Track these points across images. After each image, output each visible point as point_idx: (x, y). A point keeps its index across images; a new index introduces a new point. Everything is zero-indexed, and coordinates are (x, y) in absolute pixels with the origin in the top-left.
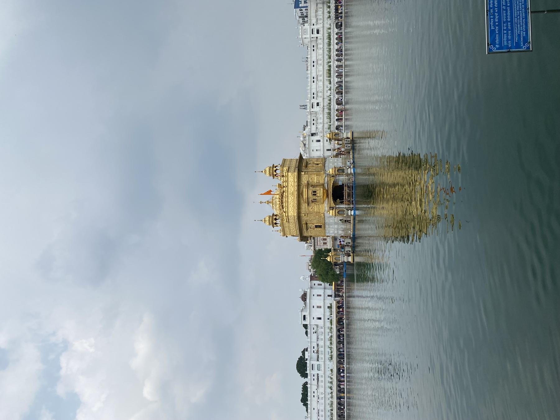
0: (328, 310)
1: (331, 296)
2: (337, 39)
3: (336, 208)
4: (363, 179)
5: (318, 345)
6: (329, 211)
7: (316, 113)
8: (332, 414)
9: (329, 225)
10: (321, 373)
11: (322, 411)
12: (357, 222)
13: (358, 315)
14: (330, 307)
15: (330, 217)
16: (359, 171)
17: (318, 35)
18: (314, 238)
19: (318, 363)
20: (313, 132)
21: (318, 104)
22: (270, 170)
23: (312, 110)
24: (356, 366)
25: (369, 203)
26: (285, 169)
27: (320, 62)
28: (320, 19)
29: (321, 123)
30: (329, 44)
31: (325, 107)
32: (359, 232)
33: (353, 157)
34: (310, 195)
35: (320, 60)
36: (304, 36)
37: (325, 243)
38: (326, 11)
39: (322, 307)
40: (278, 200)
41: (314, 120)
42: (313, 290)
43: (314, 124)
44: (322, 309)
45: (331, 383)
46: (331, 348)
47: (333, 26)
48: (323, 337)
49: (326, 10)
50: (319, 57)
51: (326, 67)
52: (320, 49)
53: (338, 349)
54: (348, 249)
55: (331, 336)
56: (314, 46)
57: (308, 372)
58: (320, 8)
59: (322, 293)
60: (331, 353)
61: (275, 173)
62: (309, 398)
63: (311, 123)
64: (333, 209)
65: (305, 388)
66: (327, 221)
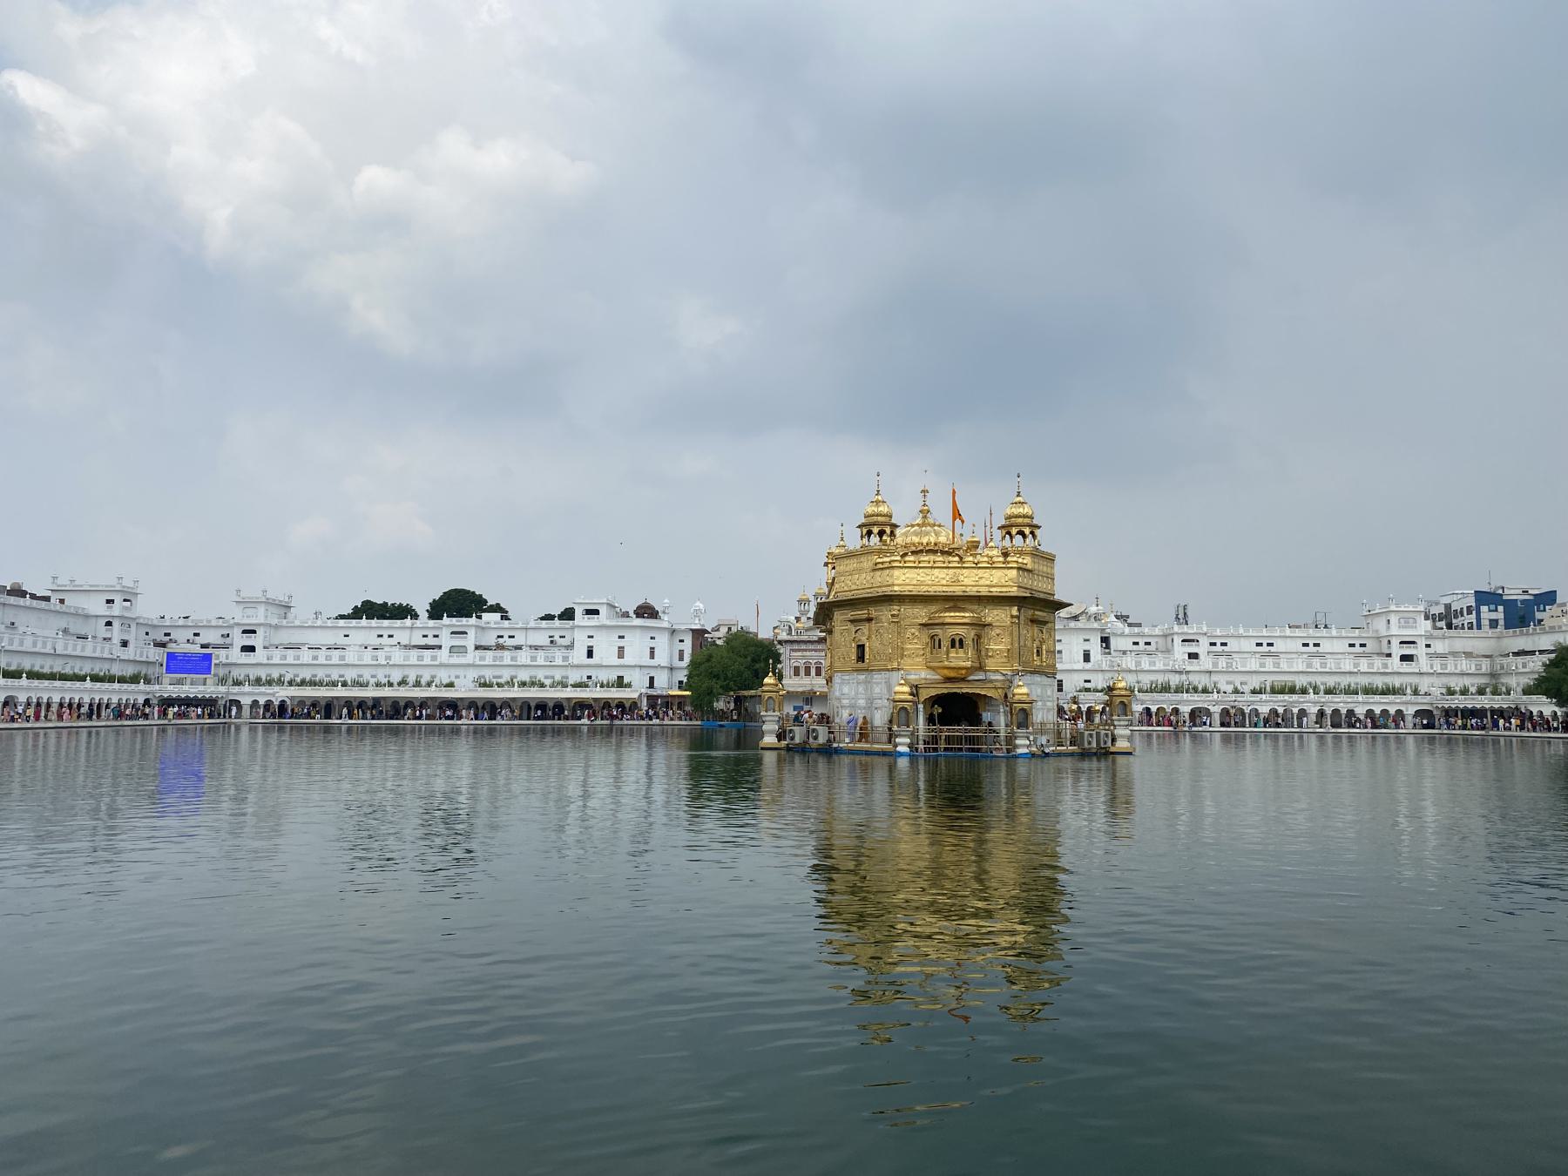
1: (651, 685)
2: (1385, 712)
3: (916, 704)
4: (997, 784)
5: (518, 648)
6: (907, 683)
7: (1168, 651)
8: (334, 684)
9: (866, 682)
10: (443, 656)
11: (342, 658)
13: (601, 757)
14: (620, 683)
15: (889, 688)
16: (1022, 768)
17: (1396, 659)
18: (822, 640)
19: (471, 648)
20: (1113, 642)
22: (1025, 516)
23: (1178, 640)
24: (463, 750)
26: (1027, 560)
27: (1317, 664)
28: (1444, 666)
29: (1138, 663)
30: (1369, 691)
31: (1184, 677)
33: (1060, 755)
35: (1323, 665)
36: (1394, 619)
37: (797, 672)
38: (1467, 681)
39: (621, 661)
40: (933, 540)
41: (1148, 644)
43: (1136, 643)
44: (616, 661)
45: (418, 684)
46: (510, 683)
47: (1423, 703)
48: (540, 661)
49: (1472, 683)
50: (1334, 661)
51: (1301, 681)
52: (1356, 665)
53: (507, 703)
55: (542, 685)
56: (1362, 645)
58: (1478, 667)
60: (499, 685)
61: (1014, 531)
62: (374, 622)
63: (1138, 635)
64: (912, 694)
65: (402, 612)
66: (877, 677)
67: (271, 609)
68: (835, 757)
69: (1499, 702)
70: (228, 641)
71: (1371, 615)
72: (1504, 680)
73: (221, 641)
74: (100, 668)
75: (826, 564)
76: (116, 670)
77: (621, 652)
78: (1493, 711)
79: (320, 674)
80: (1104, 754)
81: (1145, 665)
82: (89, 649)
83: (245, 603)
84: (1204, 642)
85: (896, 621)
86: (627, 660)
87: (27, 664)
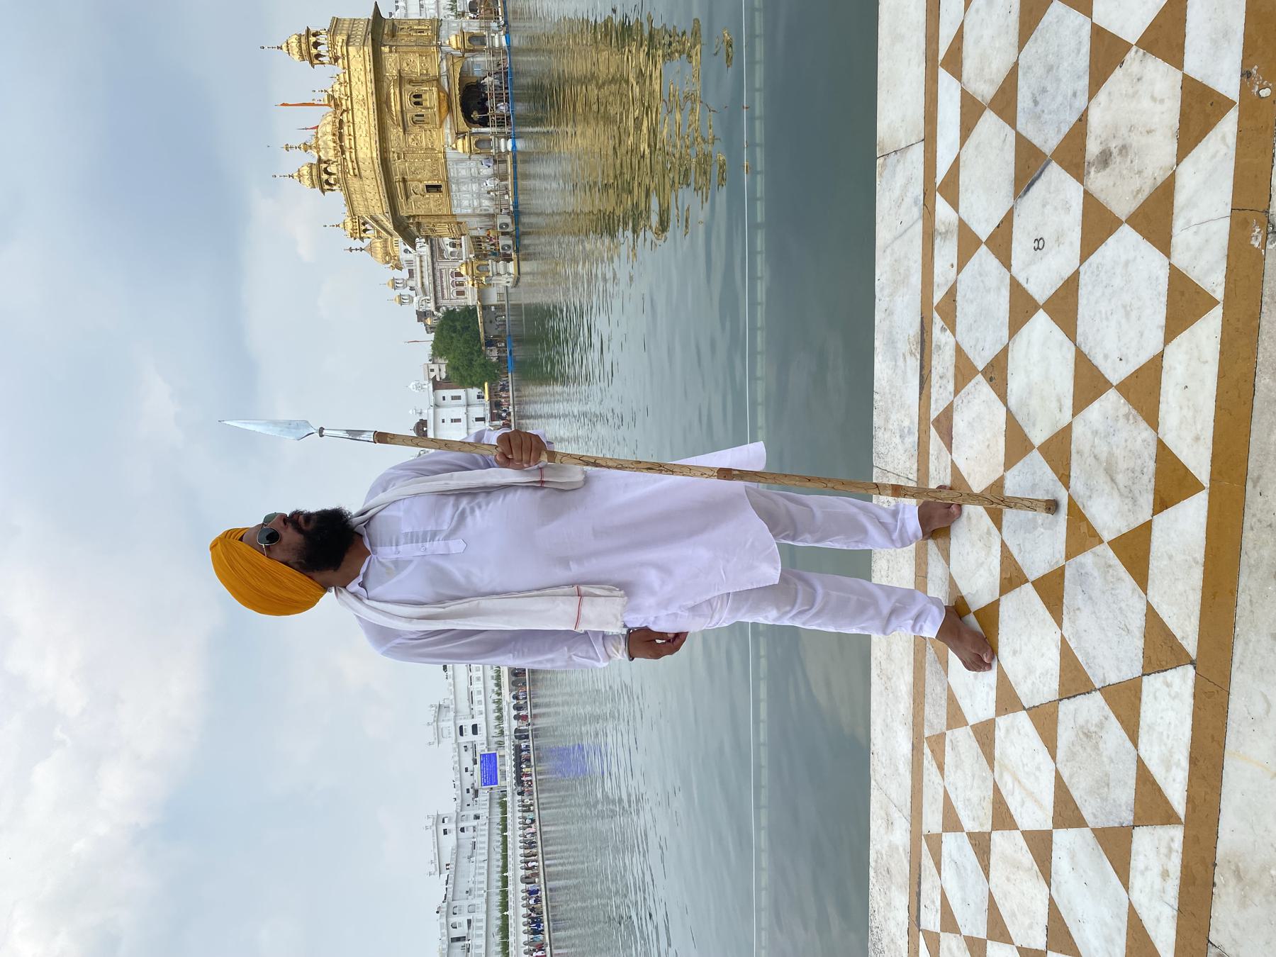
1: (483, 419)
3: (472, 134)
9: (458, 184)
18: (427, 237)
22: (300, 42)
34: (408, 104)
37: (461, 293)
40: (330, 137)
42: (439, 410)
61: (314, 51)
68: (520, 208)
70: (469, 746)
73: (470, 751)
74: (497, 829)
76: (497, 818)
82: (482, 840)
85: (402, 155)
87: (496, 876)
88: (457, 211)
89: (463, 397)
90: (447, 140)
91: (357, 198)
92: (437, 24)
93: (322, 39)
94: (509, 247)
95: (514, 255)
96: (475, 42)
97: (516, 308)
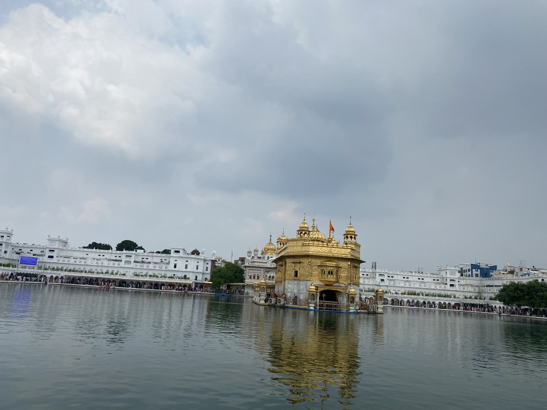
0: (182, 275)
1: (196, 279)
2: (445, 303)
3: (317, 293)
4: (342, 321)
5: (150, 263)
7: (374, 278)
8: (82, 272)
9: (298, 284)
10: (122, 264)
11: (85, 262)
12: (294, 310)
13: (176, 303)
14: (185, 277)
15: (306, 287)
16: (352, 317)
18: (276, 268)
19: (132, 262)
21: (382, 280)
22: (352, 232)
23: (377, 275)
24: (127, 299)
25: (320, 325)
26: (353, 246)
27: (423, 285)
28: (464, 289)
30: (440, 296)
32: (291, 314)
34: (329, 269)
35: (425, 286)
36: (448, 272)
37: (250, 277)
38: (471, 294)
39: (186, 270)
40: (317, 236)
42: (203, 261)
43: (363, 275)
45: (112, 273)
46: (146, 275)
47: (457, 301)
48: (157, 268)
49: (473, 295)
51: (418, 291)
52: (436, 287)
53: (144, 283)
54: (273, 300)
55: (157, 277)
56: (438, 280)
57: (124, 251)
58: (475, 290)
59: (199, 270)
60: (142, 276)
61: (349, 236)
63: (364, 272)
65: (107, 247)
66: (302, 282)
67: (60, 243)
69: (481, 302)
70: (43, 253)
71: (440, 270)
72: (483, 295)
73: (40, 253)
75: (278, 242)
77: (186, 267)
78: (480, 305)
79: (77, 268)
80: (375, 313)
81: (367, 283)
83: (51, 240)
84: (386, 275)
85: (310, 264)
86: (188, 269)
88: (287, 282)
89: (207, 272)
90: (313, 283)
91: (295, 243)
92: (357, 284)
93: (353, 240)
94: (271, 302)
95: (267, 304)
96: (351, 299)
97: (241, 300)
